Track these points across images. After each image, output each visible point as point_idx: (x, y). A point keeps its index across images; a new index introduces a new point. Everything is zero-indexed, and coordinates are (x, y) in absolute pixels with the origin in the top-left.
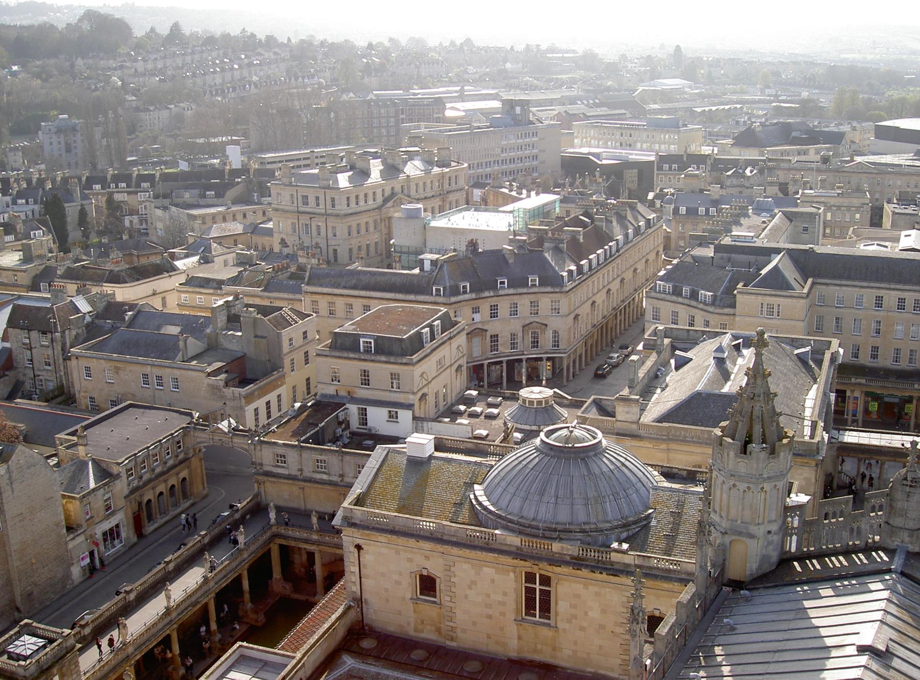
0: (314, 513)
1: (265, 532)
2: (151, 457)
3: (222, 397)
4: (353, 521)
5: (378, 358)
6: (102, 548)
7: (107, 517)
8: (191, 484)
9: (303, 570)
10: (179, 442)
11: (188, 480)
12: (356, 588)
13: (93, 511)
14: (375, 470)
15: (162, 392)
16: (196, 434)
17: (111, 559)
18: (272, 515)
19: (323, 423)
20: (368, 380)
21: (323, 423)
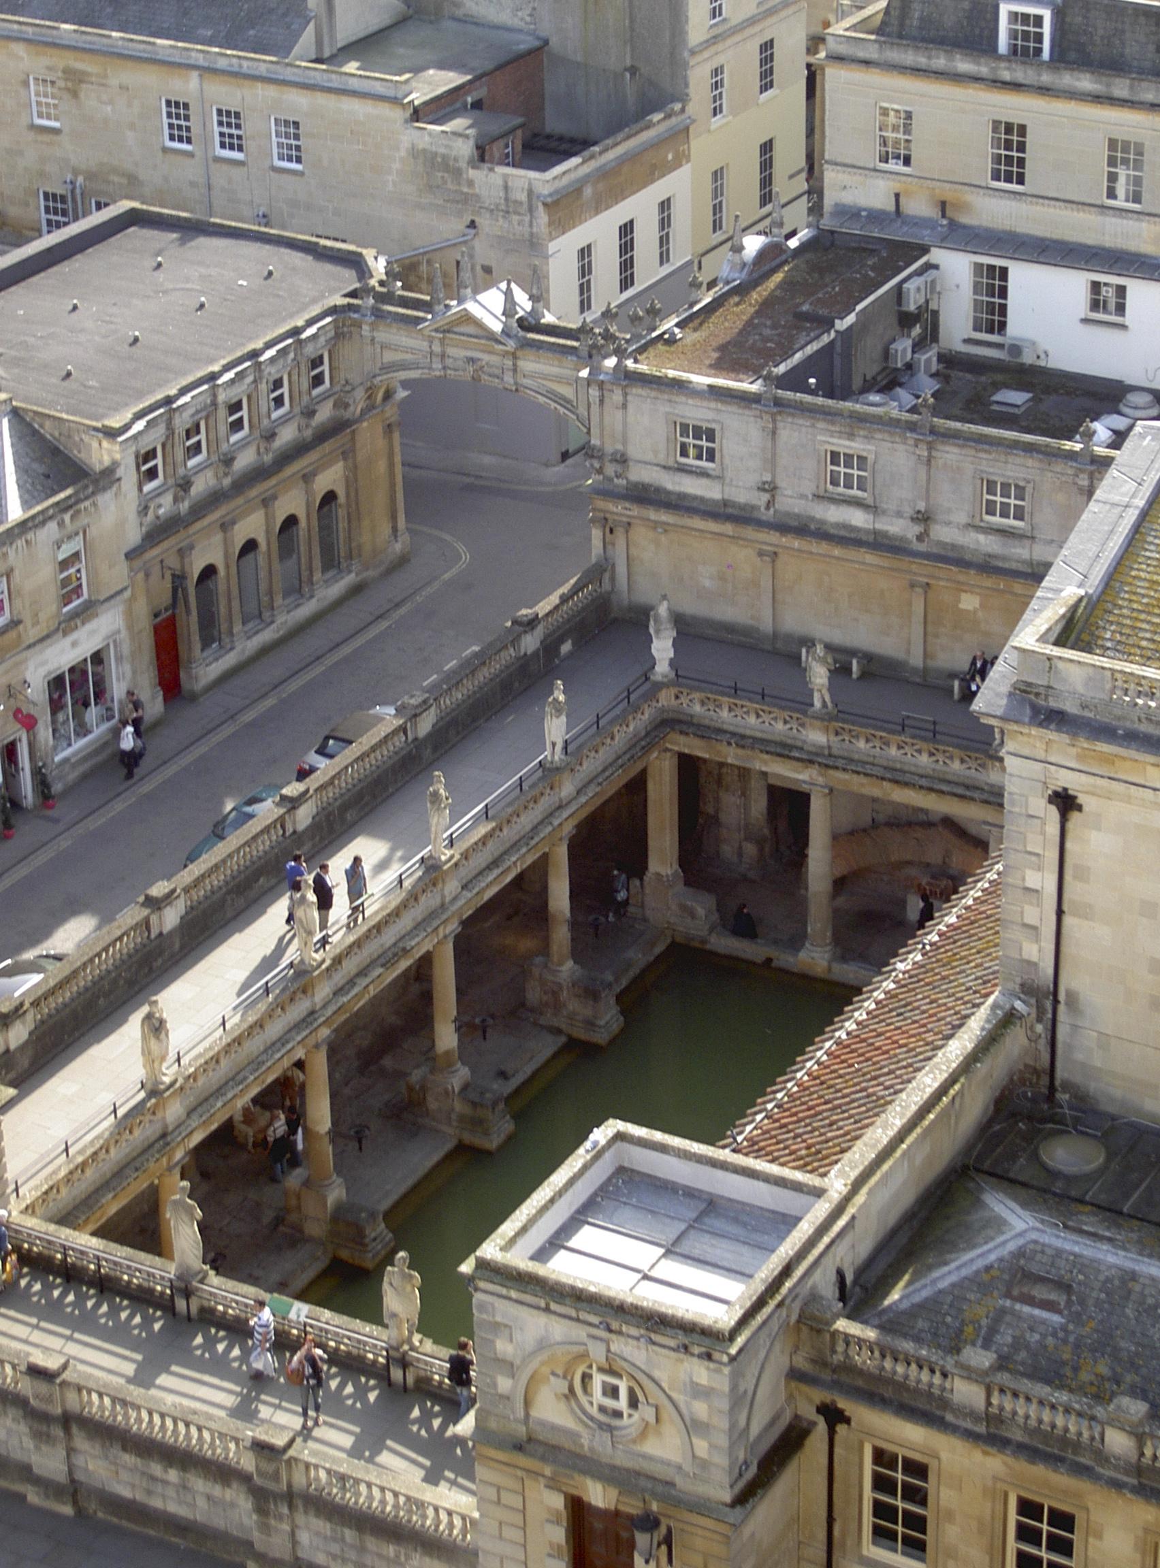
0: (820, 650)
1: (636, 709)
2: (222, 412)
3: (466, 199)
4: (1053, 704)
5: (1068, 79)
6: (44, 733)
7: (67, 625)
8: (354, 516)
9: (750, 849)
10: (317, 362)
11: (342, 498)
12: (1039, 952)
13: (18, 603)
14: (1131, 516)
15: (236, 172)
16: (383, 335)
17: (72, 776)
18: (662, 649)
19: (851, 319)
20: (1021, 162)
21: (851, 319)
